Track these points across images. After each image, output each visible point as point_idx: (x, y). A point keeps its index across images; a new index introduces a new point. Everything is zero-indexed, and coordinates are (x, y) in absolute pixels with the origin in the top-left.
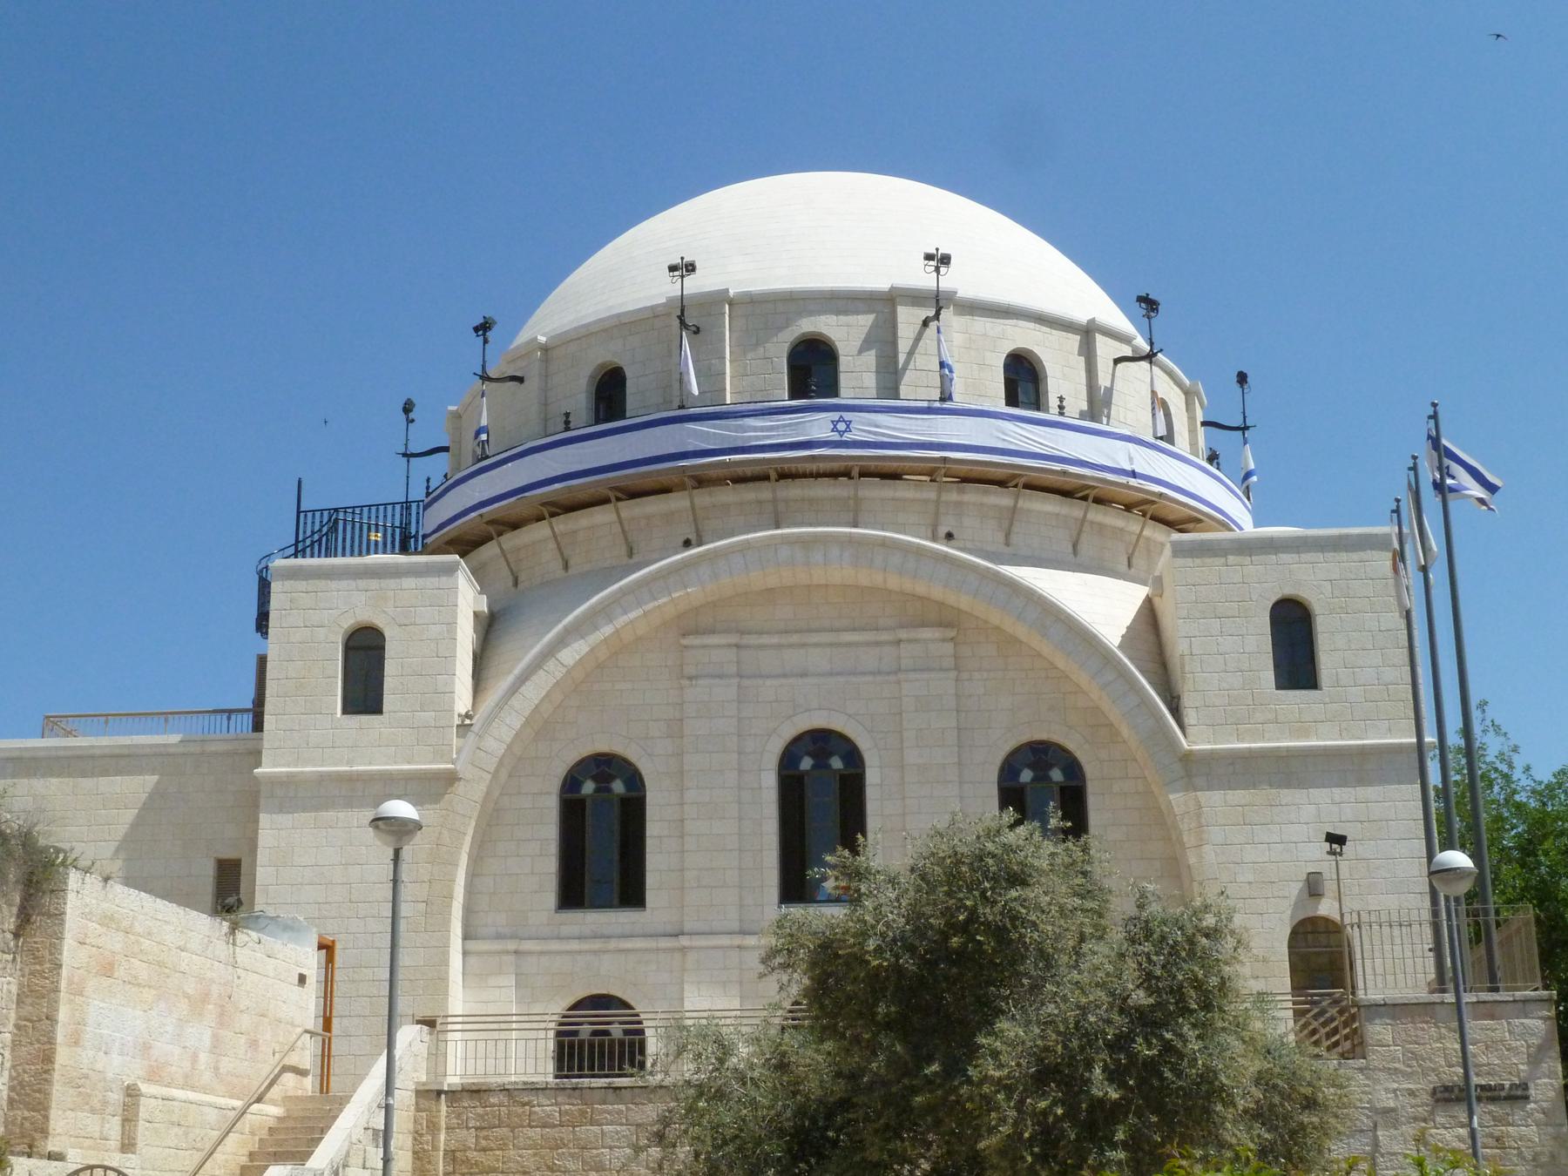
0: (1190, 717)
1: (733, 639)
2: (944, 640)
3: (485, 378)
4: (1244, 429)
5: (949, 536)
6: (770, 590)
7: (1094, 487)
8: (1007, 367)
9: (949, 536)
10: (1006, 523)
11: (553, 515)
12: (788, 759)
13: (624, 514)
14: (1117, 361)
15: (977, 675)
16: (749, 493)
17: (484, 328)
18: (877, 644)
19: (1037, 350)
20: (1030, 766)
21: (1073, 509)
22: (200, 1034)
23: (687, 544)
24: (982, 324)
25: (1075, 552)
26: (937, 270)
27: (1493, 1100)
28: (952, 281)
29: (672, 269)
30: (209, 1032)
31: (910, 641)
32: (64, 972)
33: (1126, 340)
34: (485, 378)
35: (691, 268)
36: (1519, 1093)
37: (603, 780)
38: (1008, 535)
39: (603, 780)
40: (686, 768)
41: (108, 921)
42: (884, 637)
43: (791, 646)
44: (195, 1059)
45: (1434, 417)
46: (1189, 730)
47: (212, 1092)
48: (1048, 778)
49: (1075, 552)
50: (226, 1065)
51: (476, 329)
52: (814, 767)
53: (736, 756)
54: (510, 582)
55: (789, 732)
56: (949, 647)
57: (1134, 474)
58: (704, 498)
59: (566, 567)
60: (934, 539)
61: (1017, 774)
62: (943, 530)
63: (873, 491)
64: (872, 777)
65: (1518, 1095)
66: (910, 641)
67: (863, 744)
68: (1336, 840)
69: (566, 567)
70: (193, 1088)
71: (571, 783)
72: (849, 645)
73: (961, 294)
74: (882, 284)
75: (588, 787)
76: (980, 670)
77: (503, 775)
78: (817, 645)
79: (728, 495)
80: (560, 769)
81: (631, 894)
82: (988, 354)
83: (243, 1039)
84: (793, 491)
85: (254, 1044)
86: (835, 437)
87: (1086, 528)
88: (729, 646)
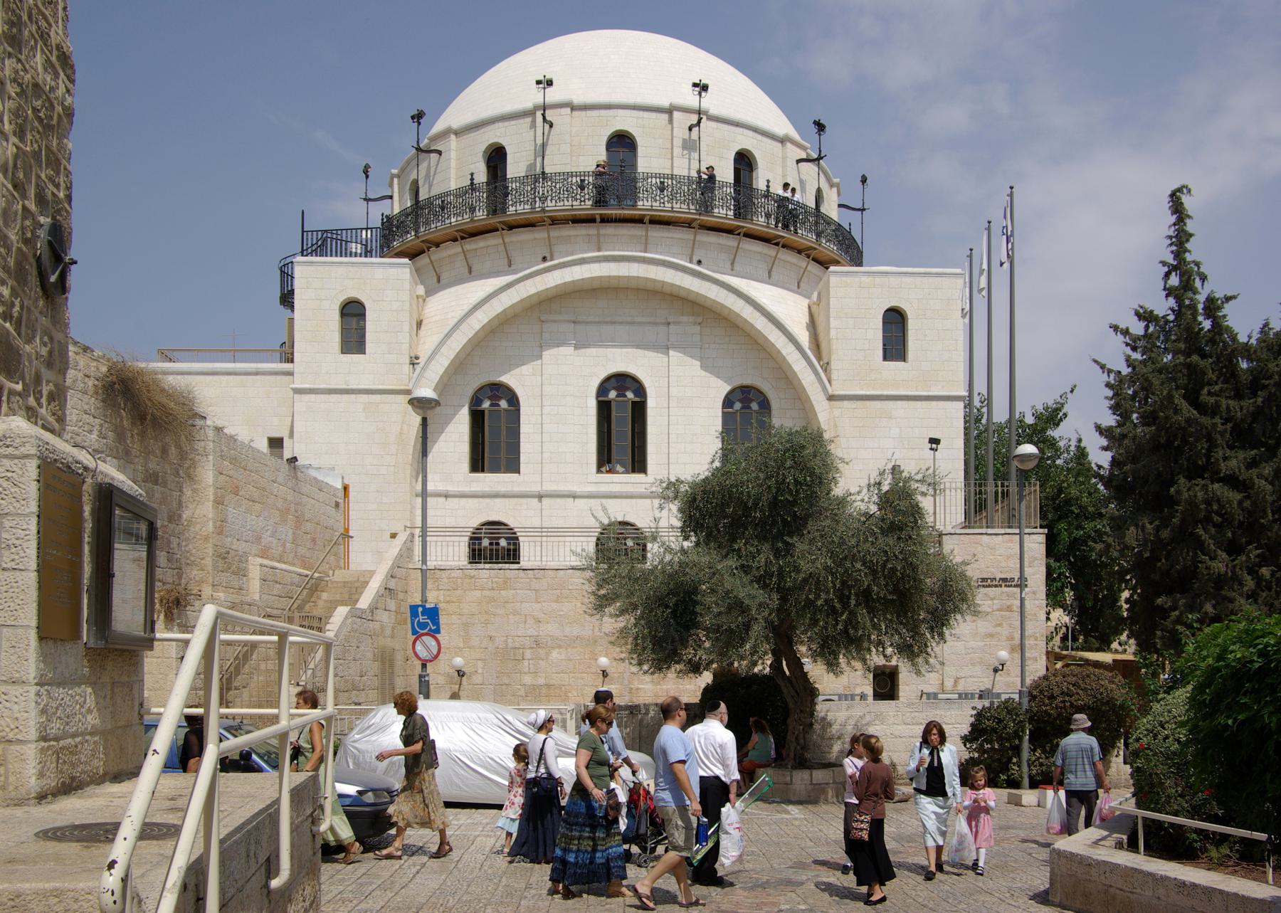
2: (695, 324)
6: (594, 290)
8: (736, 161)
9: (699, 262)
11: (463, 238)
12: (602, 389)
13: (507, 240)
18: (656, 324)
20: (740, 401)
21: (770, 251)
22: (287, 532)
23: (544, 259)
26: (700, 94)
28: (710, 102)
29: (539, 82)
30: (290, 532)
35: (550, 83)
38: (733, 264)
43: (606, 323)
44: (284, 546)
45: (1011, 195)
47: (294, 565)
54: (435, 279)
55: (603, 375)
58: (556, 232)
59: (470, 272)
60: (691, 262)
62: (695, 260)
63: (657, 233)
64: (651, 403)
68: (934, 441)
69: (470, 272)
72: (640, 323)
73: (714, 111)
74: (665, 103)
78: (621, 323)
80: (470, 392)
85: (314, 540)
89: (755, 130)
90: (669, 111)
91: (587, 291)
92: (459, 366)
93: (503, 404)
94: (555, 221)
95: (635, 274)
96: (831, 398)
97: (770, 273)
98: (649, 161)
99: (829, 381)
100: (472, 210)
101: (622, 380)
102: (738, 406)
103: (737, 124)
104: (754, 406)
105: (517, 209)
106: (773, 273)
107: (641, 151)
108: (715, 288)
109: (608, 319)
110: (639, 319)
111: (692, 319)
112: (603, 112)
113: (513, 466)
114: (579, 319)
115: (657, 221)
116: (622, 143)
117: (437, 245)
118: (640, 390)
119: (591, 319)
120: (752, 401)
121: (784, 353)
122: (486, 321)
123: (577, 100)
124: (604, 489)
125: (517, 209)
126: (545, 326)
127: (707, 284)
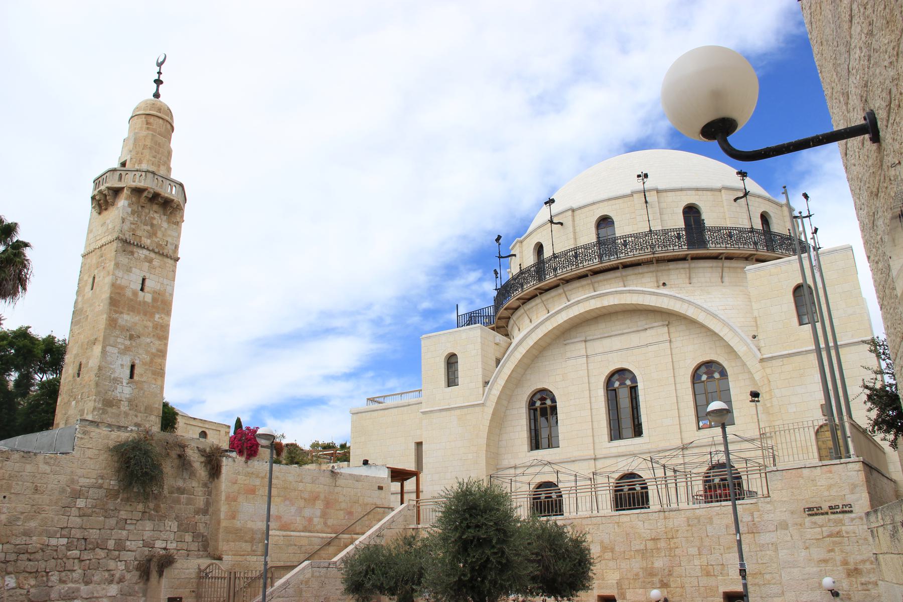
3: (500, 257)
4: (809, 216)
5: (664, 284)
9: (664, 284)
14: (735, 200)
16: (584, 282)
20: (705, 373)
27: (832, 513)
32: (223, 494)
34: (500, 257)
35: (551, 201)
36: (847, 509)
37: (543, 399)
39: (543, 399)
41: (249, 475)
44: (310, 520)
48: (713, 377)
50: (330, 522)
56: (666, 329)
62: (661, 283)
65: (846, 510)
68: (755, 395)
70: (310, 531)
71: (531, 404)
75: (538, 404)
77: (505, 403)
79: (576, 284)
81: (552, 443)
83: (342, 512)
84: (600, 277)
87: (725, 270)
89: (697, 189)
90: (632, 195)
92: (515, 381)
93: (548, 402)
94: (567, 281)
95: (612, 303)
96: (762, 360)
97: (722, 277)
98: (622, 229)
99: (759, 350)
100: (522, 285)
101: (621, 373)
102: (704, 377)
103: (681, 190)
104: (717, 375)
105: (550, 279)
106: (726, 279)
108: (666, 300)
110: (625, 331)
111: (661, 323)
113: (552, 443)
114: (588, 338)
115: (626, 266)
116: (604, 222)
117: (516, 309)
118: (634, 379)
119: (595, 337)
120: (713, 372)
123: (575, 206)
124: (614, 451)
125: (550, 279)
126: (568, 347)
127: (660, 299)
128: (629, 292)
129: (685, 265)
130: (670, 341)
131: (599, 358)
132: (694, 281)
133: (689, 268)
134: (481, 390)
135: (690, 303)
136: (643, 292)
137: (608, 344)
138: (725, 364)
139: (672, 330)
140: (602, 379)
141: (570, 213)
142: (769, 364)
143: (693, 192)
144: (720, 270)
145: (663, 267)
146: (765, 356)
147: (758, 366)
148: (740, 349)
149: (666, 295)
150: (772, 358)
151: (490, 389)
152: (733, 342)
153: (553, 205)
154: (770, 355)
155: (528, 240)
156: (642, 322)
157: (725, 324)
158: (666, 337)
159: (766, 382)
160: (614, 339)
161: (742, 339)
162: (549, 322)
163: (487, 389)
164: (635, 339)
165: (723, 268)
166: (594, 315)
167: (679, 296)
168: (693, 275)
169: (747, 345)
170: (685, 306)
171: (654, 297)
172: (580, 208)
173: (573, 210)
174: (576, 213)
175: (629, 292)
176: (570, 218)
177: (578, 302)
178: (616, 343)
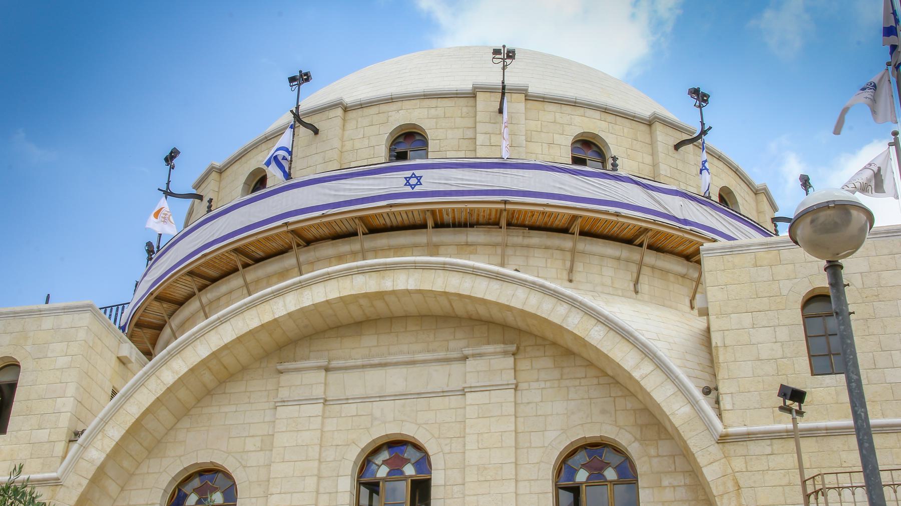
0: (726, 403)
1: (323, 362)
2: (505, 353)
3: (168, 193)
7: (647, 230)
10: (568, 264)
14: (677, 147)
15: (535, 385)
17: (171, 158)
19: (602, 134)
20: (584, 466)
24: (551, 113)
25: (637, 292)
29: (292, 79)
31: (474, 356)
33: (689, 132)
37: (203, 492)
40: (272, 476)
42: (455, 355)
46: (725, 415)
49: (637, 292)
51: (166, 160)
52: (389, 474)
53: (316, 463)
55: (365, 440)
56: (511, 360)
57: (686, 222)
61: (573, 472)
64: (437, 478)
66: (474, 356)
67: (431, 447)
73: (535, 88)
74: (468, 86)
76: (538, 380)
78: (397, 364)
79: (328, 249)
82: (556, 136)
86: (408, 189)
87: (645, 270)
88: (319, 368)
89: (606, 110)
90: (472, 95)
91: (348, 326)
96: (723, 439)
97: (636, 282)
101: (396, 445)
103: (575, 104)
104: (610, 474)
106: (644, 287)
107: (431, 143)
109: (376, 361)
111: (499, 348)
112: (384, 108)
114: (334, 364)
118: (424, 462)
119: (351, 363)
121: (636, 375)
122: (184, 370)
126: (284, 378)
128: (444, 267)
129: (566, 242)
130: (516, 389)
131: (351, 409)
132: (577, 277)
133: (573, 252)
134: (60, 447)
135: (573, 303)
136: (475, 272)
137: (374, 380)
138: (634, 450)
139: (524, 364)
140: (352, 456)
141: (339, 112)
142: (740, 448)
143: (597, 114)
144: (635, 268)
145: (517, 237)
146: (731, 430)
147: (715, 449)
148: (677, 411)
149: (523, 283)
150: (749, 437)
151: (84, 448)
152: (662, 394)
153: (304, 86)
154: (743, 429)
155: (236, 166)
156: (458, 344)
157: (647, 353)
158: (509, 377)
159: (730, 486)
160: (391, 371)
161: (681, 389)
162: (253, 312)
163: (75, 447)
164: (439, 377)
165: (641, 265)
166: (356, 313)
167: (553, 285)
168: (579, 266)
169: (693, 402)
170: (562, 309)
171: (495, 285)
172: (362, 106)
173: (346, 109)
174: (351, 115)
175: (444, 267)
176: (338, 122)
177: (328, 277)
178: (395, 380)
